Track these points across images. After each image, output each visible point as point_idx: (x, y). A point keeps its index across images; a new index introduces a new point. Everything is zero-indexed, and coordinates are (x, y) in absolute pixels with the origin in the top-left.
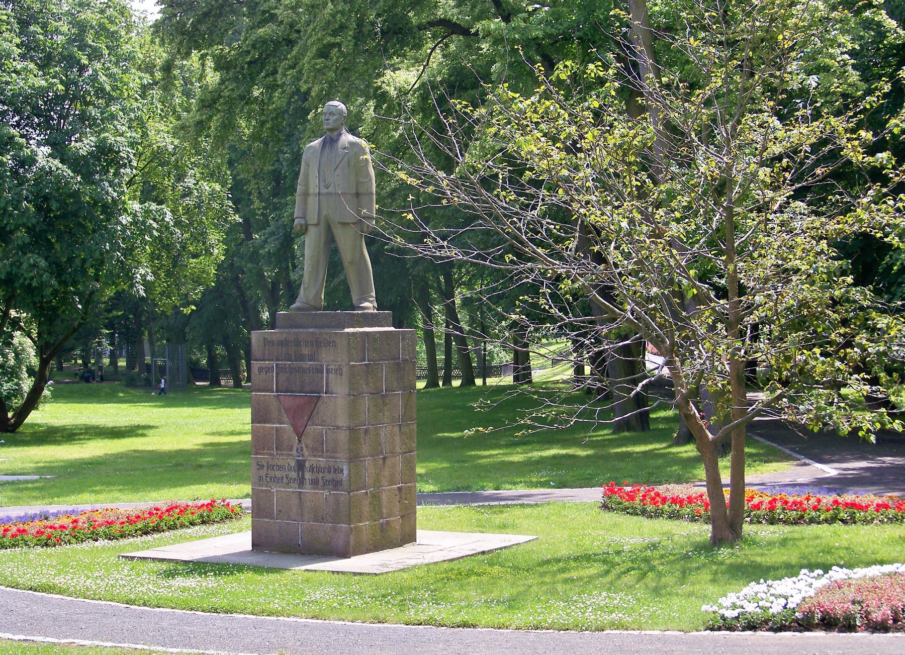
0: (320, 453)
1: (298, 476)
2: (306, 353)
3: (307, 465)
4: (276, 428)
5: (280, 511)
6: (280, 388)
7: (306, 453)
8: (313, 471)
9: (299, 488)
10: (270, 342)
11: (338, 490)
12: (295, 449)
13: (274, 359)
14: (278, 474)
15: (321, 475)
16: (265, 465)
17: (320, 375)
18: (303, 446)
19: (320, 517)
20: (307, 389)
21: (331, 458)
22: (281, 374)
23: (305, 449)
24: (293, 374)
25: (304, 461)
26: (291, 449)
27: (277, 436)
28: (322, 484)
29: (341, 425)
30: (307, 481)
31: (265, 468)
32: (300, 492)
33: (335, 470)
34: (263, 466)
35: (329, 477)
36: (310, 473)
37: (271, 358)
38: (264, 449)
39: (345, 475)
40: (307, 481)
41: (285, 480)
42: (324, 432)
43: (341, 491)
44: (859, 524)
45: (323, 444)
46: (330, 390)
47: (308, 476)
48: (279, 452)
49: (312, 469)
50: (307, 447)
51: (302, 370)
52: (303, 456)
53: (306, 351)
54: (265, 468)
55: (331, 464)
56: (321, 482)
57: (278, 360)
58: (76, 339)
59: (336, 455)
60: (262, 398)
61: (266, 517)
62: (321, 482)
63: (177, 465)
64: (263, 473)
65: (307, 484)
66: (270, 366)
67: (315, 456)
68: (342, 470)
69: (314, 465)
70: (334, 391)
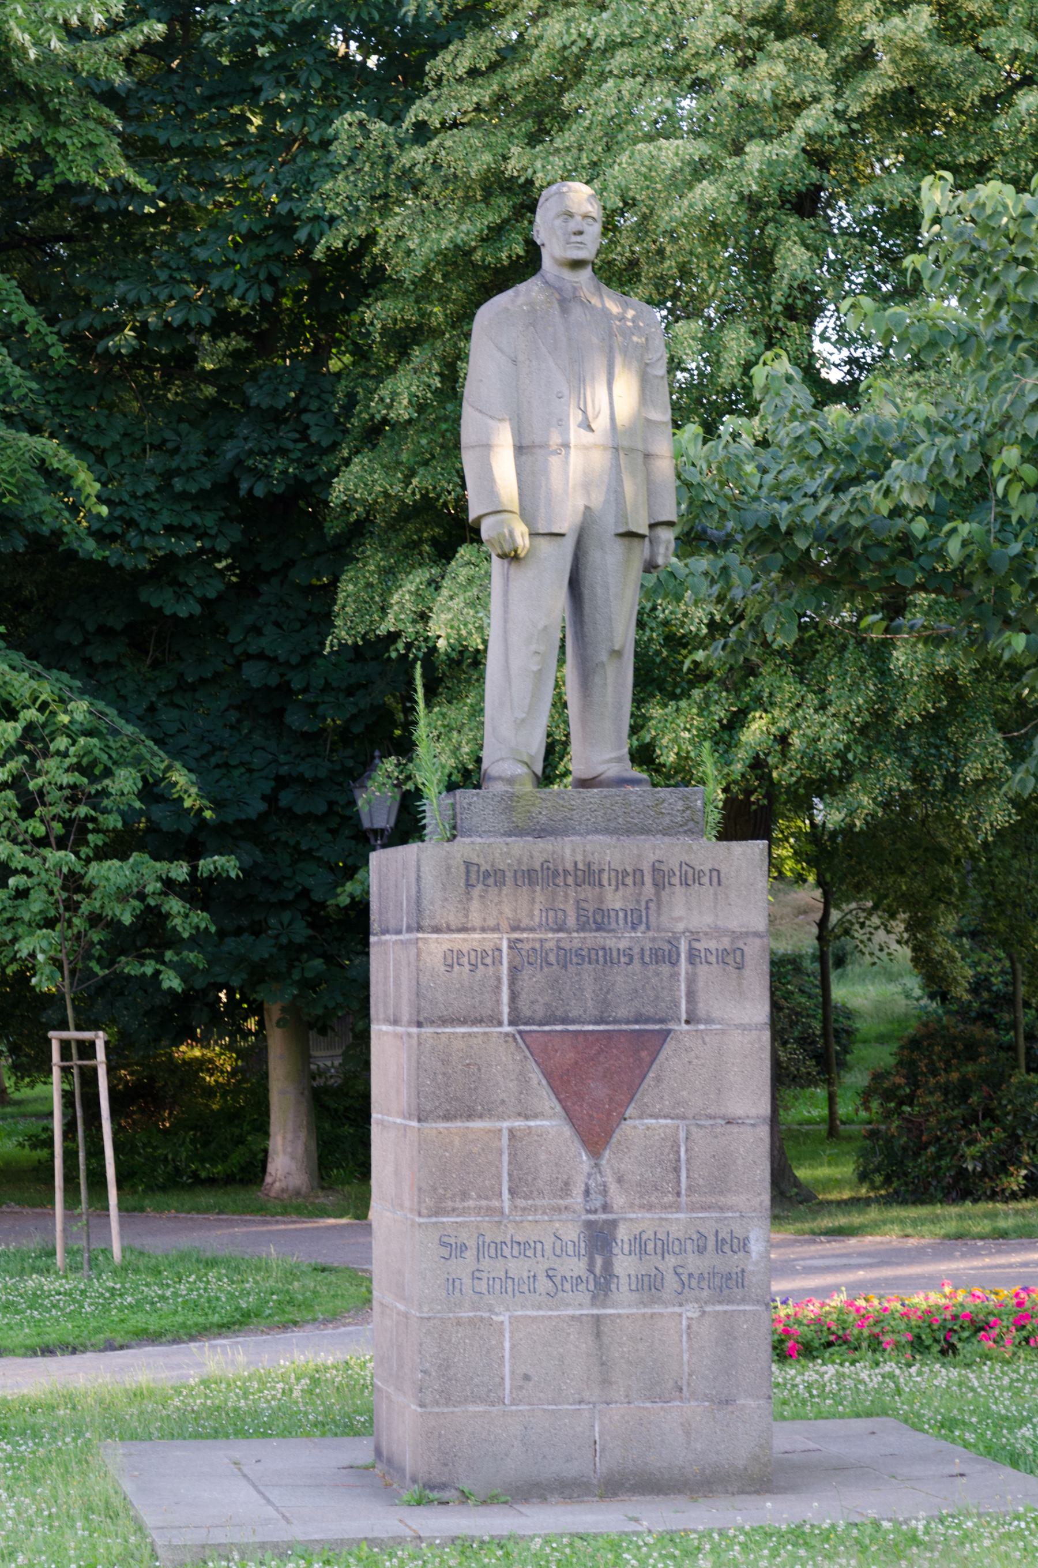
0: (669, 1198)
1: (591, 1271)
2: (618, 906)
3: (623, 1233)
4: (511, 1131)
5: (527, 1378)
6: (526, 1012)
7: (618, 1199)
8: (643, 1251)
9: (593, 1305)
10: (487, 874)
11: (730, 1302)
12: (578, 1191)
13: (504, 925)
14: (519, 1268)
15: (671, 1261)
16: (471, 1243)
17: (665, 969)
18: (610, 1179)
19: (671, 1384)
20: (622, 1012)
21: (704, 1208)
22: (527, 971)
23: (613, 1188)
24: (572, 969)
25: (614, 1224)
26: (566, 1188)
27: (513, 1156)
28: (677, 1286)
29: (740, 1112)
30: (624, 1280)
31: (470, 1255)
32: (598, 1319)
33: (720, 1245)
34: (464, 1247)
35: (694, 1263)
36: (634, 1258)
37: (491, 923)
38: (464, 1195)
39: (754, 1256)
40: (624, 1280)
41: (543, 1284)
42: (682, 1135)
43: (743, 1301)
44: (608, 1199)
45: (677, 1170)
46: (702, 1010)
47: (624, 1265)
48: (521, 1203)
49: (639, 1247)
50: (620, 1180)
51: (608, 958)
52: (606, 1208)
53: (615, 900)
54: (470, 1255)
55: (708, 1229)
56: (671, 1282)
57: (514, 929)
58: (948, 1030)
59: (722, 1200)
60: (458, 1044)
61: (477, 1399)
62: (671, 1282)
63: (323, 1270)
64: (463, 1267)
65: (623, 1291)
66: (488, 946)
67: (650, 1207)
68: (744, 1245)
69: (649, 1234)
70: (716, 1014)
